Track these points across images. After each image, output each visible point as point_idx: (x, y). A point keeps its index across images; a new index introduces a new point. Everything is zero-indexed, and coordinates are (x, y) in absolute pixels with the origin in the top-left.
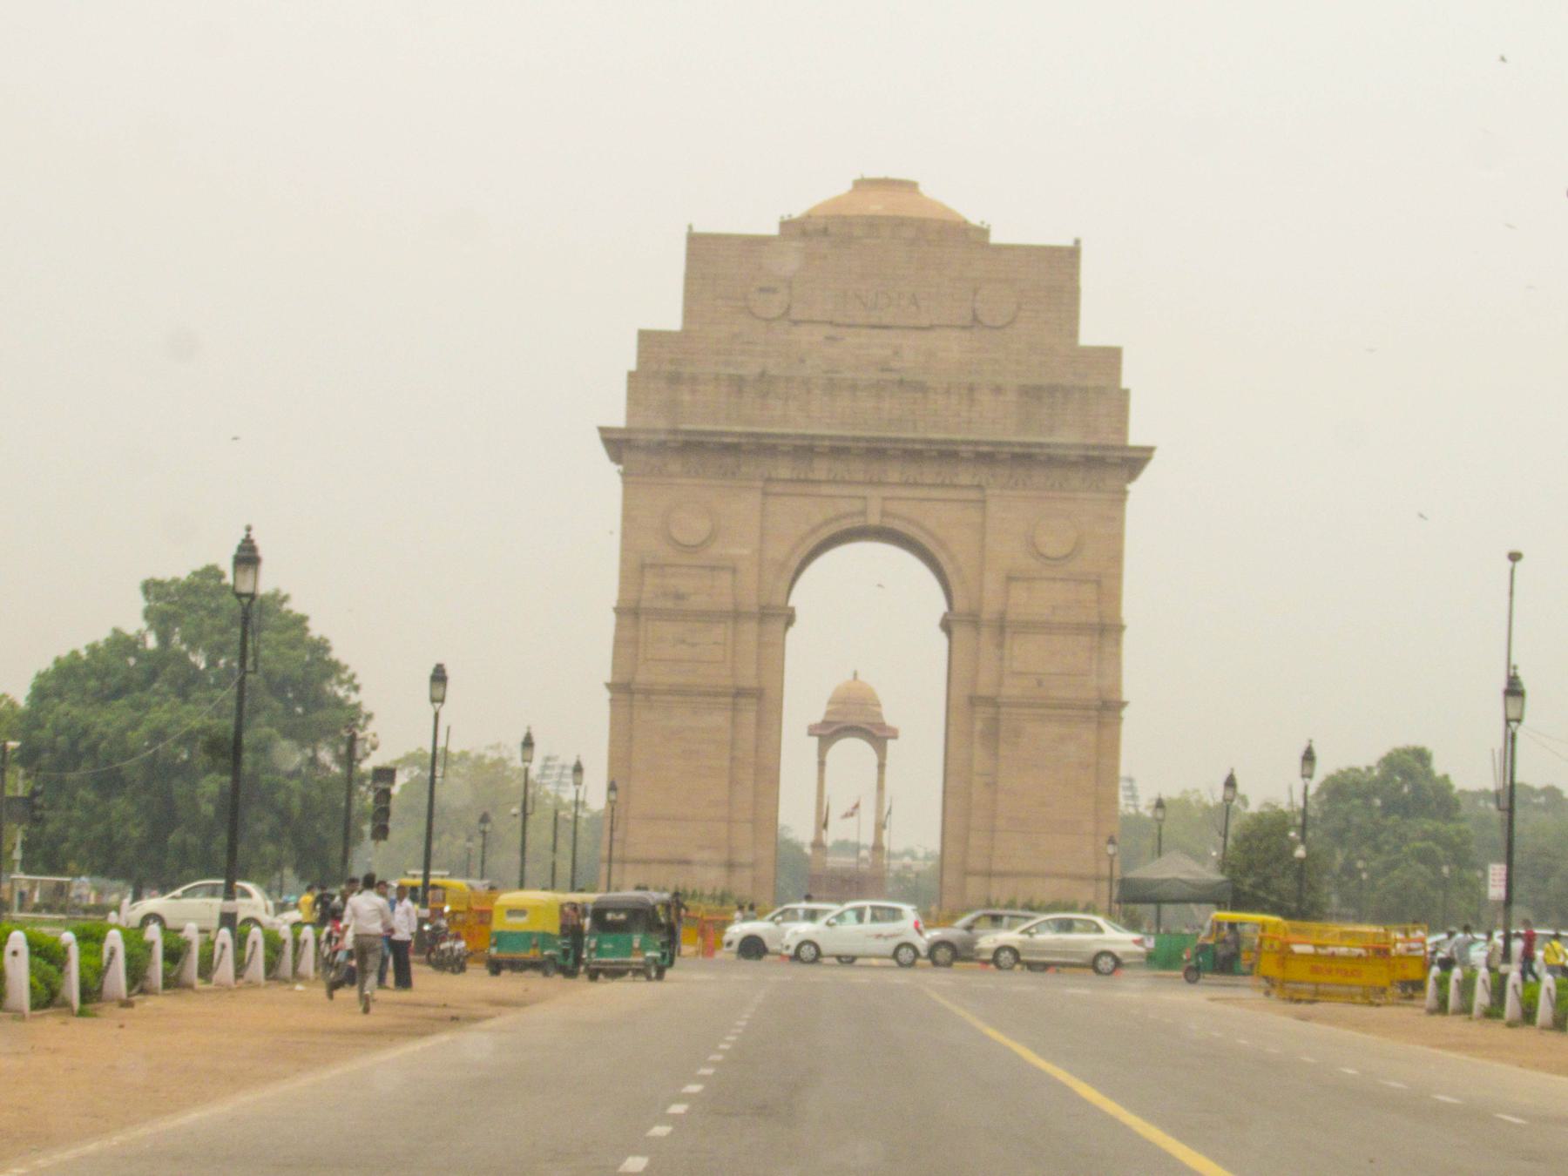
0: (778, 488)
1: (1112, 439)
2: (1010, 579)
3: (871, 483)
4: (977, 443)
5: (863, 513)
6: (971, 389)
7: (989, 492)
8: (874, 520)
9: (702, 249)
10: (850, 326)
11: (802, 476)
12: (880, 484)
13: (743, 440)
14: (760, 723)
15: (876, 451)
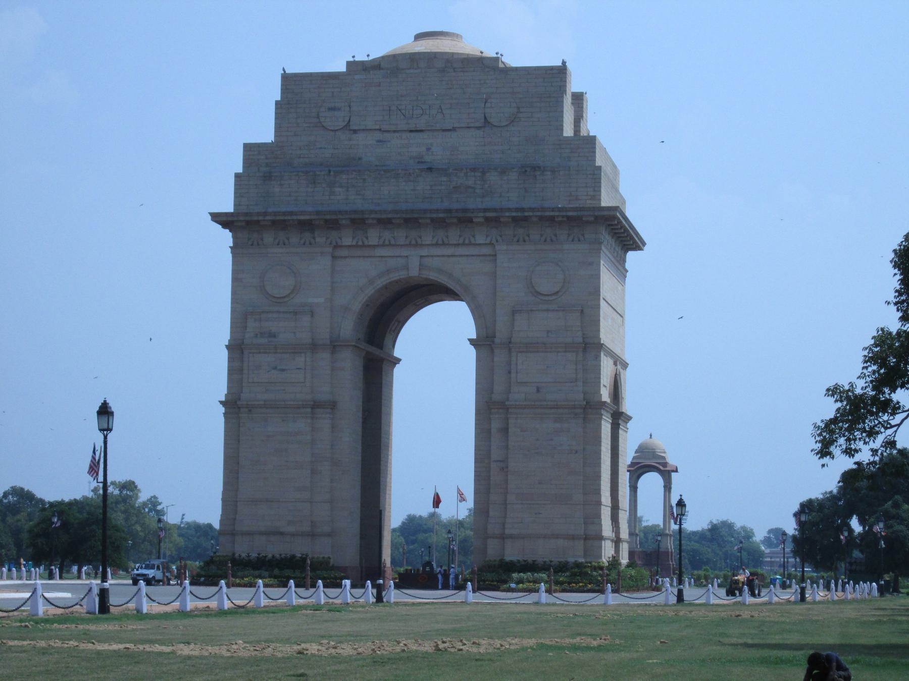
0: (344, 252)
1: (589, 203)
2: (514, 312)
3: (410, 245)
4: (485, 210)
5: (406, 267)
6: (484, 173)
7: (497, 247)
8: (414, 272)
9: (290, 82)
10: (394, 131)
11: (360, 243)
12: (417, 245)
13: (313, 217)
14: (333, 427)
15: (411, 220)
